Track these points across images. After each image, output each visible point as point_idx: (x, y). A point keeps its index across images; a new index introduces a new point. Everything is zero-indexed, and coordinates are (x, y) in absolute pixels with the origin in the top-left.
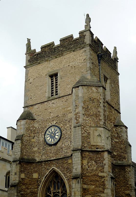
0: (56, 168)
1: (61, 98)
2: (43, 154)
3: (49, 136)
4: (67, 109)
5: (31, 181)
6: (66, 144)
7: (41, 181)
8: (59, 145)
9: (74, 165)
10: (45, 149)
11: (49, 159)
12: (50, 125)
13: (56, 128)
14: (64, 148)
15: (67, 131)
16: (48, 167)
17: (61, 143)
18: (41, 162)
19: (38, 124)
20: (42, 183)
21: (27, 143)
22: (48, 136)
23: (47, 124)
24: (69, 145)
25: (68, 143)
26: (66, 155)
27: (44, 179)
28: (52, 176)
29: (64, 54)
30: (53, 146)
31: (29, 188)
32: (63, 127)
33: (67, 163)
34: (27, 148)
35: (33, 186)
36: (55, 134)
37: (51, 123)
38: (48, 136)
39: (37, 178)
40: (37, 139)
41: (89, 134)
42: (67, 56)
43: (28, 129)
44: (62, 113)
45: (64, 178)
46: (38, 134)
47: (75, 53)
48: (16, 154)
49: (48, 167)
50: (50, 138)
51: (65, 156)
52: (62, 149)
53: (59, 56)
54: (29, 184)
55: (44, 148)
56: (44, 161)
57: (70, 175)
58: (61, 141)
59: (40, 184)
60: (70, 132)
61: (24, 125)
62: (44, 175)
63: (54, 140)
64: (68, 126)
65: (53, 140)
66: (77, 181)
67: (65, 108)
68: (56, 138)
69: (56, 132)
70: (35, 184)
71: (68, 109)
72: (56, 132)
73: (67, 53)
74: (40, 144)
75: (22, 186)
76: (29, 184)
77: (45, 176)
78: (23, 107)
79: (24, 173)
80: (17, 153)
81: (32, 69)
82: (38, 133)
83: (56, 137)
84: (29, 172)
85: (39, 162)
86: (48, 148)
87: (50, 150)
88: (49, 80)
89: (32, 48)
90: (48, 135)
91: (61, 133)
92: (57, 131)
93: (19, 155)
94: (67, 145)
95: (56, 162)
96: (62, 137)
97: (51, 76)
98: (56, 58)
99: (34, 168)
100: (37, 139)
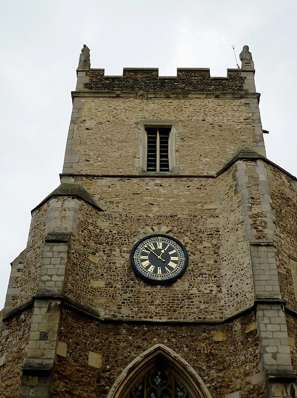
0: (170, 350)
1: (184, 179)
2: (123, 303)
3: (146, 257)
4: (202, 206)
5: (82, 371)
6: (203, 289)
7: (111, 382)
8: (179, 286)
9: (265, 342)
10: (133, 289)
11: (143, 319)
12: (150, 232)
13: (171, 243)
14: (197, 299)
15: (203, 257)
16: (140, 341)
17: (187, 284)
18: (120, 322)
19: (108, 223)
20: (115, 385)
21: (77, 258)
22: (142, 257)
23: (139, 229)
24: (214, 293)
25: (210, 288)
26: (204, 318)
27: (124, 374)
28: (144, 373)
29: (190, 96)
30: (159, 287)
31: (74, 392)
32: (191, 244)
33: (208, 339)
34: (77, 274)
35: (87, 391)
36: (167, 257)
37: (153, 229)
38: (142, 257)
39: (97, 369)
40: (105, 258)
41: (288, 271)
42: (198, 102)
43: (83, 225)
44: (186, 212)
45: (201, 381)
46: (108, 248)
47: (221, 102)
48: (48, 281)
49: (140, 341)
50: (152, 263)
51: (200, 318)
52: (190, 299)
53: (175, 95)
54: (77, 382)
55: (128, 287)
56: (130, 323)
57: (221, 374)
58: (186, 277)
59: (107, 388)
60: (216, 262)
61: (75, 210)
62: (127, 364)
63: (164, 271)
64: (205, 244)
65: (159, 271)
66: (289, 390)
67: (195, 203)
68: (171, 268)
69: (170, 253)
70: (92, 386)
71: (206, 207)
72: (170, 253)
73: (198, 96)
74: (113, 273)
75: (58, 381)
76: (77, 382)
77: (130, 365)
78: (60, 175)
79: (67, 343)
80: (51, 276)
81: (93, 103)
82: (107, 243)
83: (171, 264)
84: (78, 344)
85: (107, 321)
86: (143, 290)
87: (149, 294)
88: (144, 137)
89: (93, 66)
90: (144, 254)
91: (187, 257)
92: (175, 251)
93: (60, 284)
94: (208, 291)
95: (171, 333)
96: (190, 268)
97: (151, 130)
98: (168, 97)
99: (91, 335)
100: (105, 258)
